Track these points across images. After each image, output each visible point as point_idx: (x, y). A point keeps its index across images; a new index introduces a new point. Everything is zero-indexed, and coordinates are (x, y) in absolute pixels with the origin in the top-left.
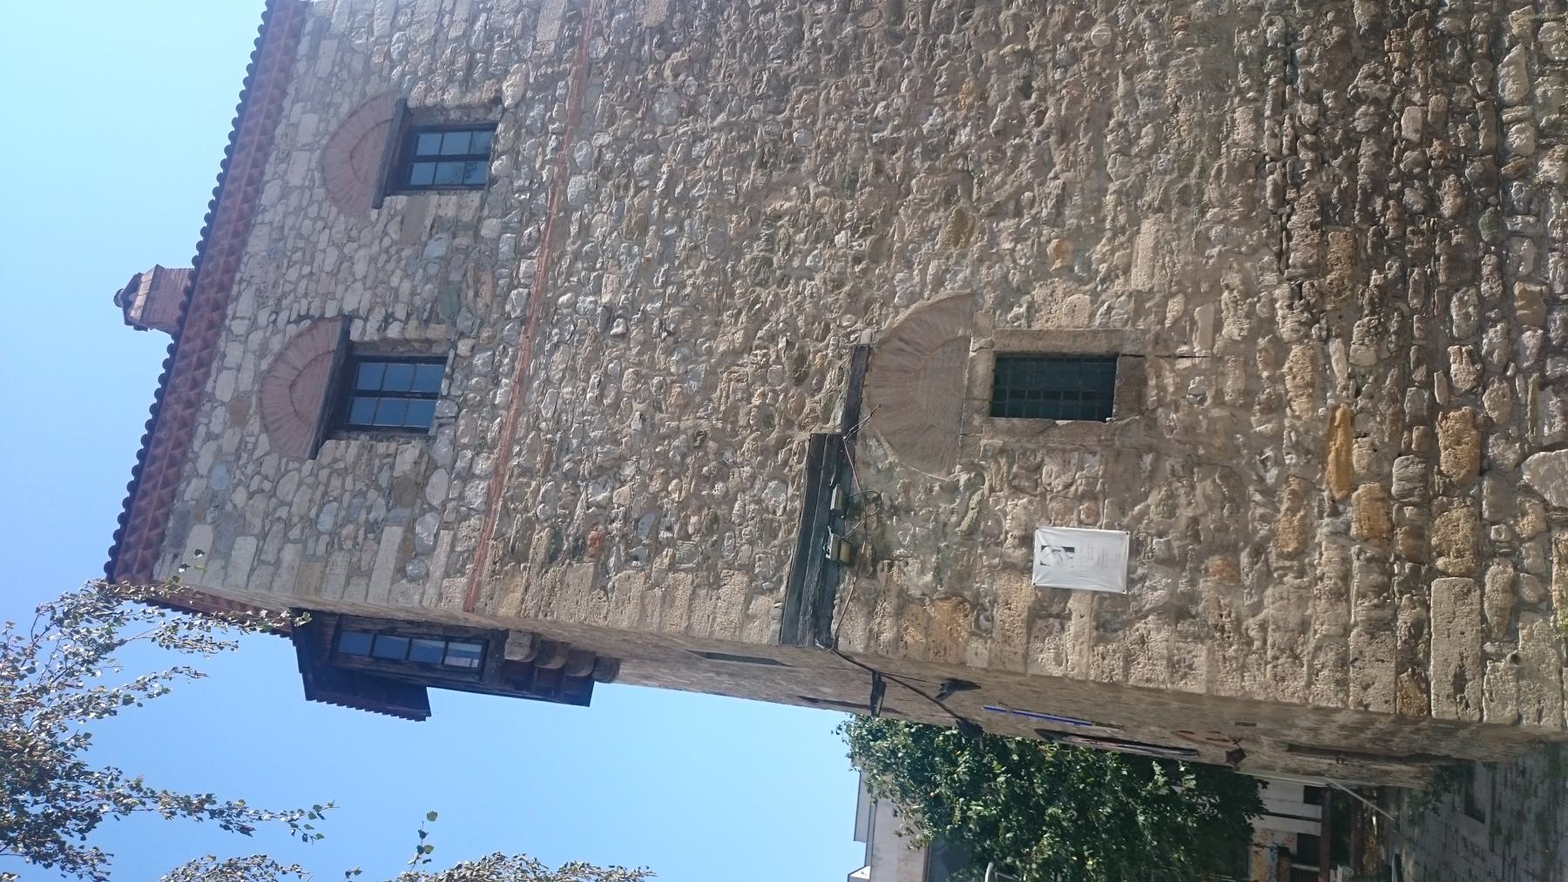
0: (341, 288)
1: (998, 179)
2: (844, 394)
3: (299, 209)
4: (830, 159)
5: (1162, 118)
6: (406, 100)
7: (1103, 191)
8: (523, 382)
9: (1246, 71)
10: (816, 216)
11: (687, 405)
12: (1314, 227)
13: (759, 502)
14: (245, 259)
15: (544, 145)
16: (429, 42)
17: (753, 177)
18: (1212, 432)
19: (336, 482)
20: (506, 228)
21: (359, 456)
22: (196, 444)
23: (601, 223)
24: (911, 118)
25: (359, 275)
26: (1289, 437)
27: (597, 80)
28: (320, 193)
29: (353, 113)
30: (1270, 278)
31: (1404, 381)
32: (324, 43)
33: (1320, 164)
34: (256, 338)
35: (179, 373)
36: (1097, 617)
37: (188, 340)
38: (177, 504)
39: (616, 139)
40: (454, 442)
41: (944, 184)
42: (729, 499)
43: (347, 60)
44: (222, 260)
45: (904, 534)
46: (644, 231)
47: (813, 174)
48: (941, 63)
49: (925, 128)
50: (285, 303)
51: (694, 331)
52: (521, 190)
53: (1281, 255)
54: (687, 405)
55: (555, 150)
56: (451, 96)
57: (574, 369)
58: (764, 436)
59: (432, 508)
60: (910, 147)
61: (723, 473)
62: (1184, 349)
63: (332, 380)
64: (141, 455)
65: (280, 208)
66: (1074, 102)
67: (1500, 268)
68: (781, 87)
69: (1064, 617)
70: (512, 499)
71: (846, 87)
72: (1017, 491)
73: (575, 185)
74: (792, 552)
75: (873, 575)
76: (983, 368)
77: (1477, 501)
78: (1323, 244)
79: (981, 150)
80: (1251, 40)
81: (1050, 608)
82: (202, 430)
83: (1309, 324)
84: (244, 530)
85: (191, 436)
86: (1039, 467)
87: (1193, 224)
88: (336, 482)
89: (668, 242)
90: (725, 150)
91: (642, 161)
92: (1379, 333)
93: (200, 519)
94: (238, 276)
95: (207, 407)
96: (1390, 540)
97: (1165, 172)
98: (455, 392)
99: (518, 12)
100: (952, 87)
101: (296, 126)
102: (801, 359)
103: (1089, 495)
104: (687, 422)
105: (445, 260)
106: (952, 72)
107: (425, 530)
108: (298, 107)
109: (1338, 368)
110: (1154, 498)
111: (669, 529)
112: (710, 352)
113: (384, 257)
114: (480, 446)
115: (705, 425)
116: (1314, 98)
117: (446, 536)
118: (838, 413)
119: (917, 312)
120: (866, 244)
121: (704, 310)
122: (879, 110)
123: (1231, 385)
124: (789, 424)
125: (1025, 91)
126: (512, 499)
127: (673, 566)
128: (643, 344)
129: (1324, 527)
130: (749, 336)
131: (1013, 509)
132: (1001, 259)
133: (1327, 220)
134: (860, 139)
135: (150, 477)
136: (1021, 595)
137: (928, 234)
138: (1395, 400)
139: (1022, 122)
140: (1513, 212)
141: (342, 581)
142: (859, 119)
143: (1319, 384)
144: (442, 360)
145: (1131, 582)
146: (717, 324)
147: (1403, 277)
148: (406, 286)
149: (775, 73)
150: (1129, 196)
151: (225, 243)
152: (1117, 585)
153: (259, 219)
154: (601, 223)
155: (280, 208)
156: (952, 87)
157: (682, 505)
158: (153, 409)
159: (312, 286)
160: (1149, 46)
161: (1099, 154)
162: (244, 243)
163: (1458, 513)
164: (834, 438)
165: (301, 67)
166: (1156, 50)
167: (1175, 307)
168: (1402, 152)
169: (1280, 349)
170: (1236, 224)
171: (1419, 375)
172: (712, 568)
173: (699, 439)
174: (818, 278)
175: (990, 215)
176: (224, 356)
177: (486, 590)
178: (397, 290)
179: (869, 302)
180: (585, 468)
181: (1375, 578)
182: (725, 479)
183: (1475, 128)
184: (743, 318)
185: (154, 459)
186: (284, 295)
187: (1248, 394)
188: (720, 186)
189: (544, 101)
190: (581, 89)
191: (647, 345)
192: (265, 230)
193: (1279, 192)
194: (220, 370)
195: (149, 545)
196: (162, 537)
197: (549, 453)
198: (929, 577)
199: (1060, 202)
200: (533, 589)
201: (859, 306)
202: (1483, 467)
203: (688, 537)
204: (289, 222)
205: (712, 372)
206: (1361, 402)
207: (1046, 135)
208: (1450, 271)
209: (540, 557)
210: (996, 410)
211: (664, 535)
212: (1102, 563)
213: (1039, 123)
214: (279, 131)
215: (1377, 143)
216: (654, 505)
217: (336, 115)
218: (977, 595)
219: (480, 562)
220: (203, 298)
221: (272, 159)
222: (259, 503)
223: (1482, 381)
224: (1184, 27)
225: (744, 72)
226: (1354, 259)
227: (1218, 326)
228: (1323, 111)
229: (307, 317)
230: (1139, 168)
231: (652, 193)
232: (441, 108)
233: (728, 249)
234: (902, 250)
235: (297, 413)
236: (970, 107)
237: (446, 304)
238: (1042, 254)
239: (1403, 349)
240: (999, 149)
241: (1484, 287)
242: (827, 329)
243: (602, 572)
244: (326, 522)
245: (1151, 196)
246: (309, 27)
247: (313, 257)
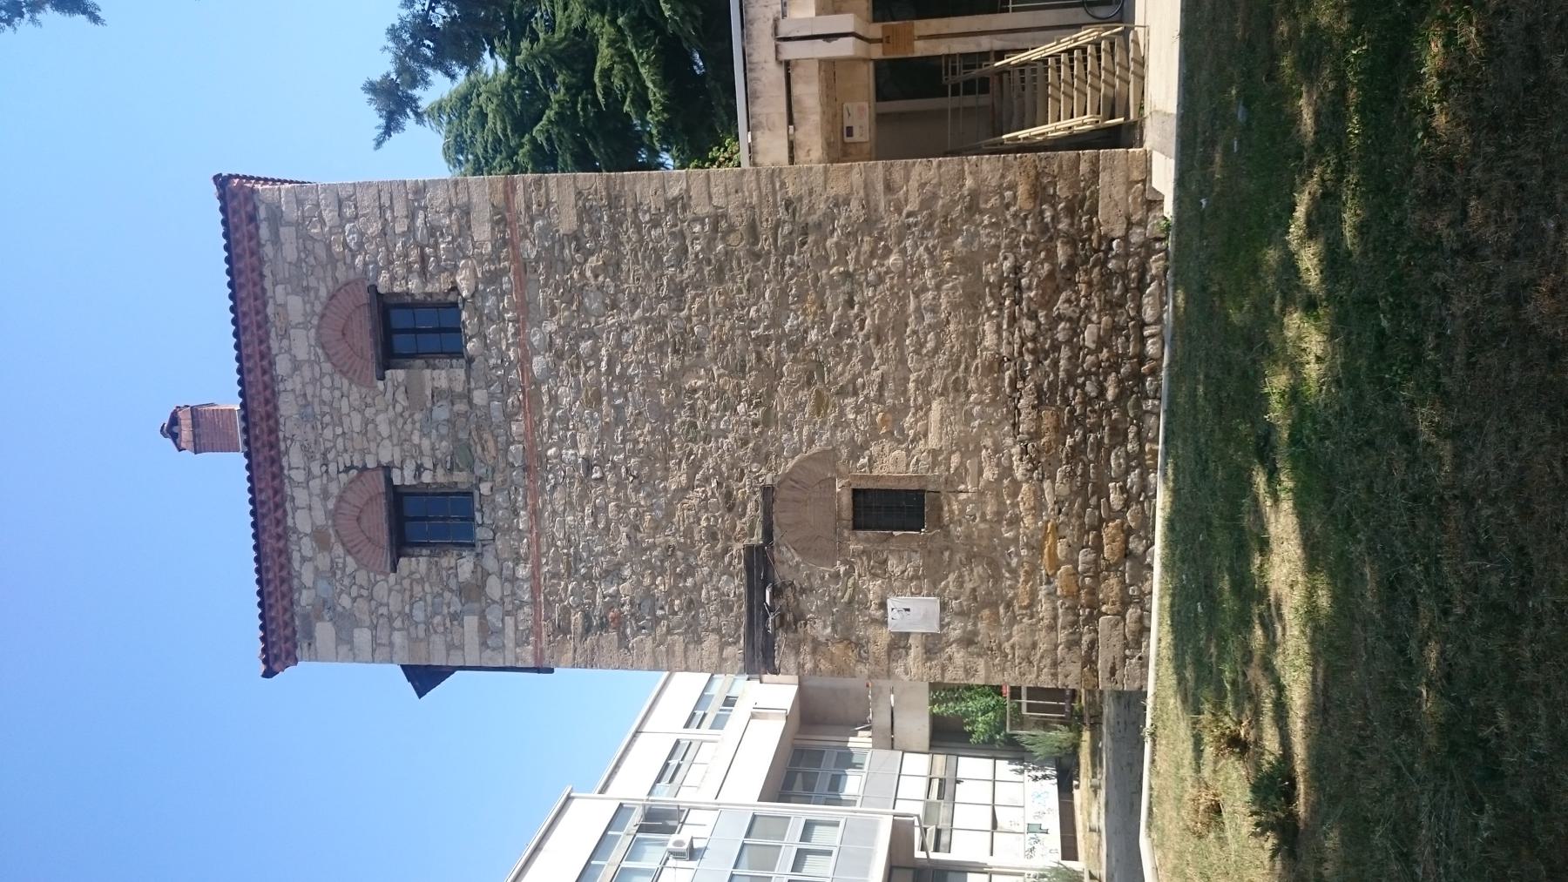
0: (373, 446)
1: (840, 368)
2: (761, 518)
3: (314, 381)
4: (722, 351)
5: (939, 327)
6: (373, 289)
7: (907, 380)
8: (536, 514)
9: (992, 294)
10: (721, 392)
11: (657, 528)
12: (1034, 407)
13: (717, 589)
14: (282, 420)
15: (506, 331)
16: (379, 235)
17: (670, 361)
18: (980, 537)
19: (417, 589)
20: (492, 397)
21: (429, 569)
22: (296, 565)
23: (565, 393)
24: (775, 322)
25: (385, 434)
26: (1023, 539)
27: (534, 277)
28: (327, 367)
29: (332, 297)
30: (1009, 441)
31: (1085, 505)
32: (282, 230)
33: (1037, 363)
34: (315, 484)
35: (264, 516)
36: (925, 647)
37: (261, 491)
38: (297, 609)
39: (561, 327)
40: (497, 557)
41: (805, 371)
42: (697, 588)
43: (310, 247)
44: (264, 426)
45: (812, 604)
46: (600, 402)
47: (714, 359)
48: (791, 278)
49: (787, 328)
50: (330, 456)
51: (651, 475)
52: (496, 367)
53: (1015, 425)
54: (657, 528)
55: (515, 334)
56: (414, 285)
57: (571, 503)
58: (713, 547)
59: (494, 602)
60: (779, 343)
61: (691, 571)
62: (962, 487)
63: (390, 515)
64: (259, 582)
65: (298, 379)
66: (883, 314)
67: (1138, 433)
68: (679, 291)
69: (907, 648)
70: (550, 593)
71: (725, 293)
72: (875, 576)
73: (538, 364)
74: (744, 620)
75: (796, 631)
76: (846, 499)
77: (1123, 573)
78: (1039, 417)
79: (826, 347)
80: (994, 271)
81: (899, 642)
82: (296, 556)
83: (1032, 471)
84: (358, 624)
85: (289, 560)
86: (885, 561)
87: (963, 405)
88: (417, 589)
89: (619, 409)
90: (648, 339)
91: (585, 346)
92: (1071, 476)
93: (320, 618)
94: (281, 435)
95: (294, 537)
96: (1078, 596)
97: (944, 368)
98: (487, 521)
99: (450, 211)
100: (801, 298)
101: (284, 306)
102: (729, 495)
103: (915, 577)
104: (660, 539)
105: (450, 422)
106: (799, 286)
107: (493, 617)
108: (280, 288)
109: (1049, 498)
110: (952, 577)
111: (662, 608)
112: (665, 489)
113: (400, 421)
114: (518, 559)
115: (672, 541)
116: (1033, 316)
117: (509, 621)
118: (759, 531)
119: (800, 461)
120: (757, 414)
121: (657, 458)
122: (752, 313)
123: (990, 509)
124: (728, 538)
125: (850, 303)
126: (550, 593)
127: (669, 632)
128: (617, 484)
129: (1043, 591)
130: (691, 478)
131: (874, 587)
132: (849, 425)
133: (1041, 402)
134: (743, 335)
135: (270, 594)
136: (883, 637)
137: (799, 407)
138: (1080, 516)
139: (851, 326)
140: (1147, 398)
141: (444, 652)
142: (739, 319)
143: (1038, 508)
144: (470, 494)
145: (942, 627)
146: (667, 469)
147: (1085, 439)
148: (426, 443)
149: (671, 279)
150: (923, 383)
151: (262, 410)
152: (935, 629)
153: (281, 387)
154: (565, 393)
155: (298, 379)
156: (801, 298)
157: (668, 593)
158: (256, 548)
159: (349, 444)
160: (928, 273)
161: (902, 353)
162: (276, 408)
163: (1113, 581)
164: (760, 548)
165: (268, 250)
166: (934, 276)
167: (955, 460)
168: (1085, 356)
169: (1016, 485)
170: (988, 405)
171: (1093, 501)
172: (695, 632)
173: (669, 551)
174: (730, 436)
175: (837, 393)
176: (293, 499)
177: (547, 653)
178: (419, 446)
179: (767, 455)
180: (596, 571)
181: (1071, 618)
182: (693, 576)
183: (1127, 338)
184: (684, 465)
185: (269, 582)
186: (327, 451)
187: (999, 514)
188: (647, 366)
189: (494, 293)
190: (521, 284)
191: (620, 485)
192: (291, 397)
193: (1013, 383)
194: (295, 509)
195: (287, 639)
196: (294, 632)
197: (568, 563)
198: (829, 630)
199: (881, 387)
200: (579, 651)
201: (762, 457)
202: (1127, 554)
203: (675, 613)
204: (309, 390)
205: (670, 503)
206: (1062, 518)
207: (867, 337)
208: (1111, 436)
209: (580, 630)
210: (856, 526)
211: (660, 613)
212: (925, 616)
213: (862, 328)
214: (270, 310)
215: (1072, 349)
216: (648, 591)
217: (317, 297)
218: (858, 638)
219: (538, 635)
220: (261, 458)
221: (273, 334)
222: (361, 603)
223: (1127, 505)
224: (950, 259)
225: (648, 276)
226: (1057, 428)
227: (980, 473)
228: (1039, 325)
229: (352, 467)
230: (927, 364)
231: (599, 371)
232: (408, 293)
233: (664, 415)
234: (784, 417)
235: (369, 539)
236: (815, 314)
237: (462, 455)
238: (873, 423)
239: (1084, 485)
240: (837, 346)
241: (1129, 447)
242: (742, 474)
243: (623, 638)
244: (419, 615)
245: (936, 384)
246: (262, 213)
247: (340, 419)
